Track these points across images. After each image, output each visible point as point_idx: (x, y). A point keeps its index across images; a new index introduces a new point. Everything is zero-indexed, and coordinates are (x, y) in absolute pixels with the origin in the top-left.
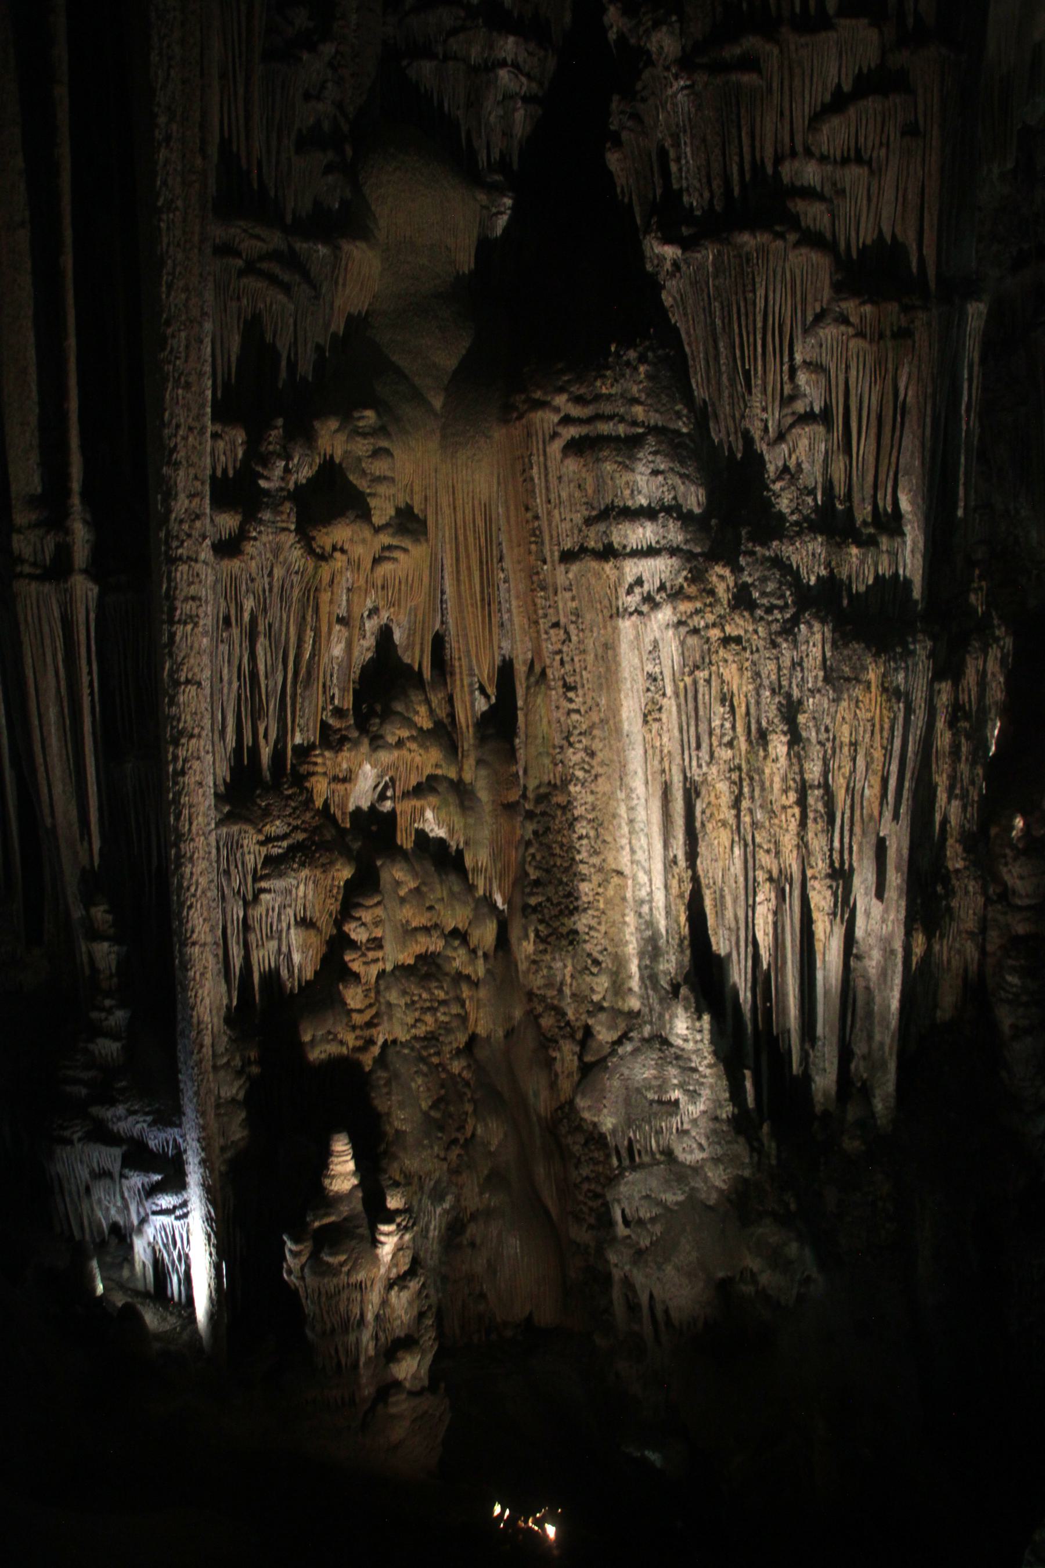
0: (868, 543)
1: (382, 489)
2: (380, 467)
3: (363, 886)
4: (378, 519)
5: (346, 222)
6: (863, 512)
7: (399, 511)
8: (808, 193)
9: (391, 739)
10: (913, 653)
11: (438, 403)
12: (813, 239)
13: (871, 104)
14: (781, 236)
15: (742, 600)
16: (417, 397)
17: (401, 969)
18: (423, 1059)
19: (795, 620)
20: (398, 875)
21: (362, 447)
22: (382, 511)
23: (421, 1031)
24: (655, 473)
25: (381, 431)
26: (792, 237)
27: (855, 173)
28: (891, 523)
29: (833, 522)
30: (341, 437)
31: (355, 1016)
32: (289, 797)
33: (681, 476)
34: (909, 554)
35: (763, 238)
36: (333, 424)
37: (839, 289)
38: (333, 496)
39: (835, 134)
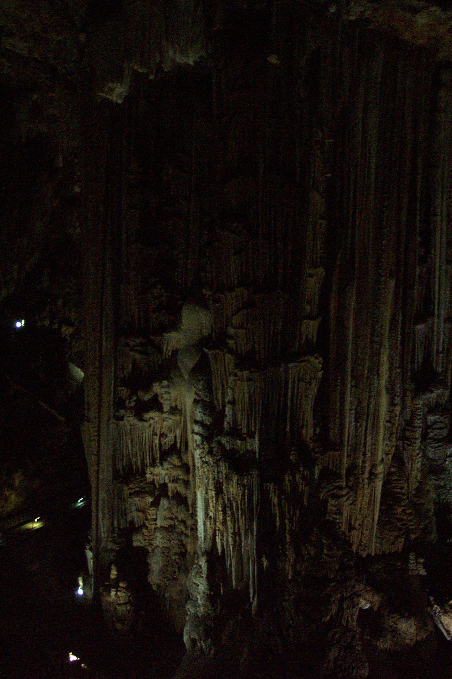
0: (243, 439)
1: (166, 402)
2: (166, 396)
3: (156, 504)
4: (165, 410)
5: (174, 325)
6: (245, 430)
7: (171, 408)
8: (231, 337)
9: (165, 467)
10: (251, 474)
11: (186, 377)
12: (231, 351)
13: (245, 311)
14: (222, 350)
15: (210, 453)
16: (181, 376)
17: (162, 528)
18: (163, 553)
19: (219, 460)
20: (164, 502)
21: (163, 390)
22: (166, 408)
23: (165, 545)
24: (200, 412)
25: (168, 387)
26: (225, 350)
27: (241, 332)
28: (251, 435)
29: (235, 433)
30: (158, 388)
31: (146, 537)
32: (138, 479)
33: (204, 414)
34: (255, 444)
35: (217, 351)
36: (157, 384)
37: (237, 366)
38: (155, 404)
39: (236, 320)
